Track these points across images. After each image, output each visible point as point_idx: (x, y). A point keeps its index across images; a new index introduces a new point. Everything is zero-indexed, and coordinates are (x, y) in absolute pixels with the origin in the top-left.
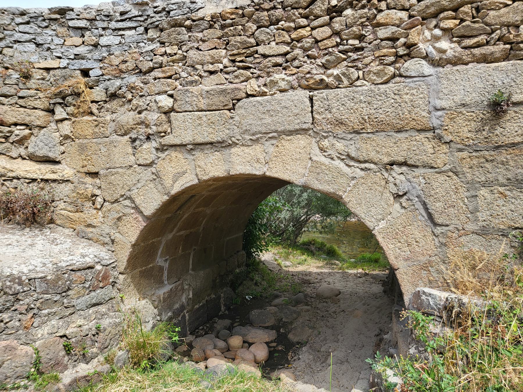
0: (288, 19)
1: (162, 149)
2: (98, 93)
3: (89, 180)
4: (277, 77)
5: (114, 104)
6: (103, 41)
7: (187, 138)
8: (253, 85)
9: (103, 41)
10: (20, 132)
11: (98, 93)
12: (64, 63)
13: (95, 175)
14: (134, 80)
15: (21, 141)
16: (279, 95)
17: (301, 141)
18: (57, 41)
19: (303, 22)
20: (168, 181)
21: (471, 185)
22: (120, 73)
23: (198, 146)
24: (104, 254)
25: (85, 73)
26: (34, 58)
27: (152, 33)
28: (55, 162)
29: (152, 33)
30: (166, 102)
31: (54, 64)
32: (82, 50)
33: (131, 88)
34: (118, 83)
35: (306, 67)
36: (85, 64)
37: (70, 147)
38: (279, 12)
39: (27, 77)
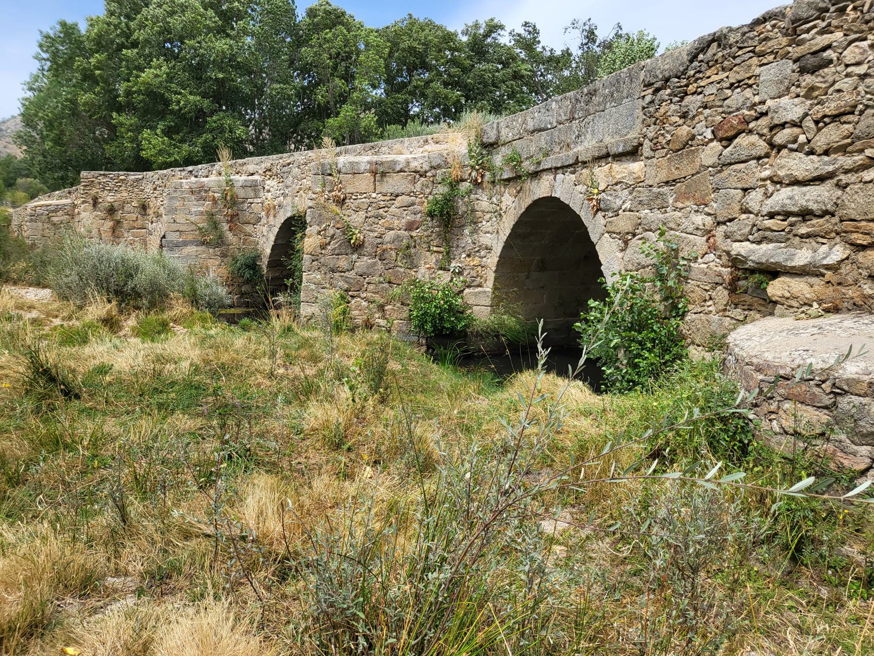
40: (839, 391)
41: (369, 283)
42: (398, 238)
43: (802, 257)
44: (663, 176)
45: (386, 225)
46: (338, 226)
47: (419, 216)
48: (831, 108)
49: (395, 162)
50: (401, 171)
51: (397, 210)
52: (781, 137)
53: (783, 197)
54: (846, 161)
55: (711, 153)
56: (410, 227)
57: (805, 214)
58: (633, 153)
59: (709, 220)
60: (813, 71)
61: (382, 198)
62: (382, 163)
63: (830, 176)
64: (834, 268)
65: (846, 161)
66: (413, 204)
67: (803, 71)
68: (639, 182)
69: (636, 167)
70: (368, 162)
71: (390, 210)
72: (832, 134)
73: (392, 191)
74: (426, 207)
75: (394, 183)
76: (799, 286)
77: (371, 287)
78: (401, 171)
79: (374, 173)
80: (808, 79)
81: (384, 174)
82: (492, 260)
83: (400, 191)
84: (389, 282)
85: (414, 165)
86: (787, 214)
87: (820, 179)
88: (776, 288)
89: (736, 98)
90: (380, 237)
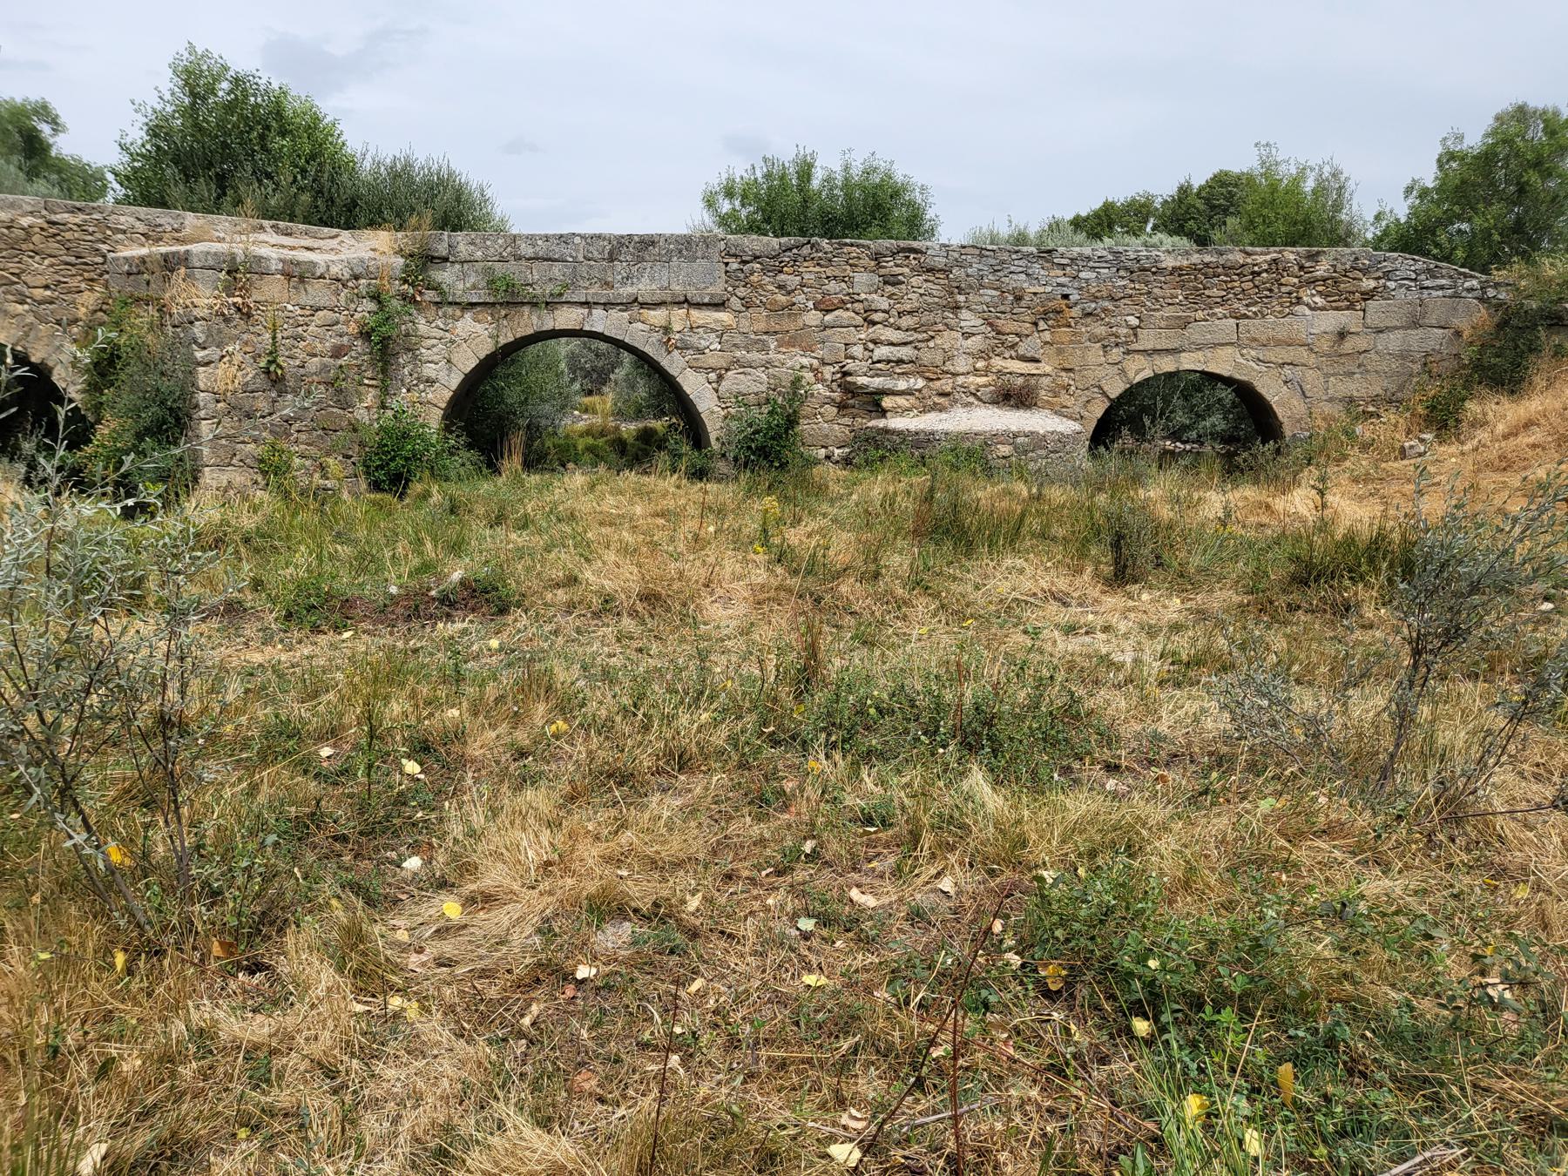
0: (1226, 275)
1: (1128, 352)
2: (1076, 312)
3: (1063, 374)
4: (1216, 310)
5: (1089, 320)
6: (1082, 275)
7: (1149, 346)
8: (1200, 315)
9: (1082, 275)
10: (1012, 339)
11: (1076, 312)
12: (1049, 289)
13: (1070, 370)
14: (1107, 304)
15: (1013, 346)
16: (1217, 322)
17: (1229, 350)
18: (1042, 272)
19: (1235, 277)
20: (1131, 374)
21: (1327, 375)
22: (1095, 299)
23: (1156, 351)
24: (1077, 427)
25: (1066, 297)
26: (1025, 285)
27: (1122, 273)
28: (1038, 361)
29: (1122, 273)
30: (1134, 321)
31: (1041, 290)
32: (1061, 280)
33: (1105, 310)
34: (1093, 305)
35: (1236, 306)
36: (1066, 291)
37: (1051, 350)
38: (1220, 270)
39: (1018, 299)
40: (1015, 436)
41: (299, 431)
42: (325, 368)
43: (902, 385)
44: (762, 326)
45: (308, 349)
46: (248, 349)
47: (345, 339)
48: (908, 307)
49: (314, 264)
50: (322, 277)
51: (319, 330)
52: (877, 317)
53: (882, 352)
54: (920, 337)
55: (813, 318)
56: (337, 352)
57: (900, 362)
58: (719, 305)
59: (815, 362)
60: (893, 284)
61: (299, 312)
62: (298, 264)
63: (911, 342)
64: (919, 391)
65: (920, 337)
66: (337, 323)
67: (886, 283)
68: (727, 329)
69: (724, 316)
70: (281, 260)
71: (311, 328)
72: (907, 321)
73: (312, 303)
74: (353, 328)
75: (317, 293)
76: (901, 401)
77: (303, 437)
78: (322, 277)
79: (288, 276)
80: (889, 289)
81: (302, 279)
82: (442, 395)
83: (322, 303)
84: (324, 429)
85: (334, 270)
86: (889, 362)
87: (905, 344)
88: (887, 402)
89: (832, 286)
90: (303, 367)
